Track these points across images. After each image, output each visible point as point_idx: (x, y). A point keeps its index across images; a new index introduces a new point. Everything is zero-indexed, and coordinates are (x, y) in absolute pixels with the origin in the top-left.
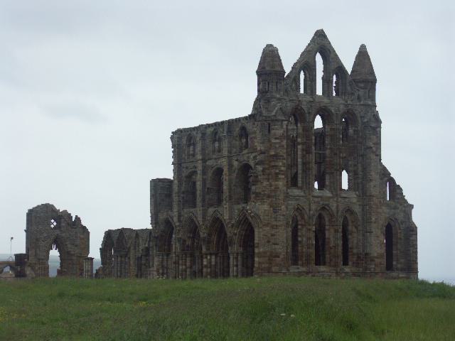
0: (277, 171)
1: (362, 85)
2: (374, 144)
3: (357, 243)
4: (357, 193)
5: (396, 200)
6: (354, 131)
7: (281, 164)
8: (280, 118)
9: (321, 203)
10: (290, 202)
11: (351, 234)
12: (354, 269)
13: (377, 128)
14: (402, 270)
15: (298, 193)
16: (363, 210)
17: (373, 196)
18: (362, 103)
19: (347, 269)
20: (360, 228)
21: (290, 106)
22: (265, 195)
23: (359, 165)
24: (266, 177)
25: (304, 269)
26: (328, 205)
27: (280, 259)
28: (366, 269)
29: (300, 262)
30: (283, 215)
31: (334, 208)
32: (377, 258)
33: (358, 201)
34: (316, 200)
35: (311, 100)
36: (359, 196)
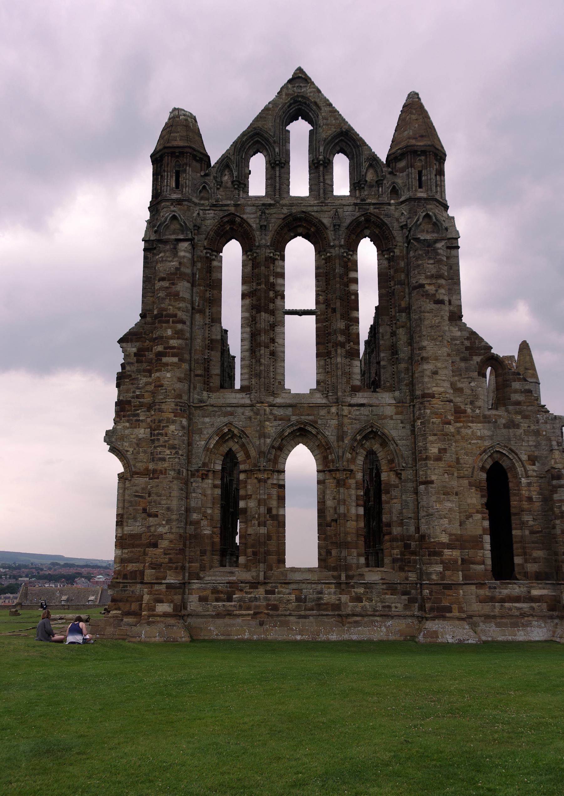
0: (160, 348)
1: (402, 164)
2: (427, 277)
3: (401, 513)
4: (397, 393)
5: (510, 408)
6: (389, 260)
7: (169, 332)
8: (173, 237)
9: (294, 418)
10: (207, 420)
11: (388, 492)
12: (397, 577)
13: (436, 241)
14: (539, 577)
15: (235, 401)
16: (413, 432)
17: (432, 396)
18: (403, 199)
19: (373, 576)
20: (408, 474)
21: (211, 219)
22: (141, 405)
23: (401, 332)
24: (145, 365)
25: (247, 576)
26: (313, 424)
27: (159, 551)
28: (421, 575)
29: (242, 560)
30: (173, 447)
31: (330, 434)
32: (449, 546)
33: (397, 413)
34: (279, 412)
35: (272, 202)
36: (399, 402)
